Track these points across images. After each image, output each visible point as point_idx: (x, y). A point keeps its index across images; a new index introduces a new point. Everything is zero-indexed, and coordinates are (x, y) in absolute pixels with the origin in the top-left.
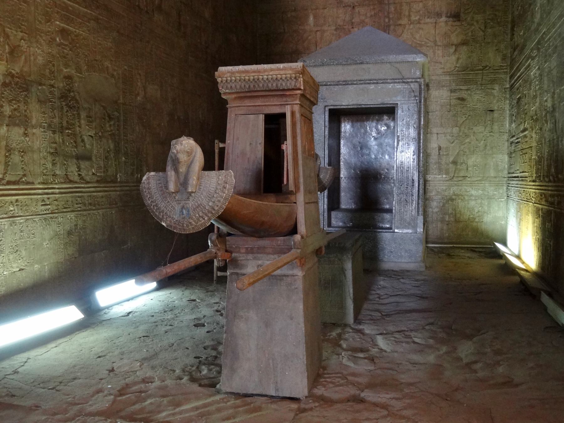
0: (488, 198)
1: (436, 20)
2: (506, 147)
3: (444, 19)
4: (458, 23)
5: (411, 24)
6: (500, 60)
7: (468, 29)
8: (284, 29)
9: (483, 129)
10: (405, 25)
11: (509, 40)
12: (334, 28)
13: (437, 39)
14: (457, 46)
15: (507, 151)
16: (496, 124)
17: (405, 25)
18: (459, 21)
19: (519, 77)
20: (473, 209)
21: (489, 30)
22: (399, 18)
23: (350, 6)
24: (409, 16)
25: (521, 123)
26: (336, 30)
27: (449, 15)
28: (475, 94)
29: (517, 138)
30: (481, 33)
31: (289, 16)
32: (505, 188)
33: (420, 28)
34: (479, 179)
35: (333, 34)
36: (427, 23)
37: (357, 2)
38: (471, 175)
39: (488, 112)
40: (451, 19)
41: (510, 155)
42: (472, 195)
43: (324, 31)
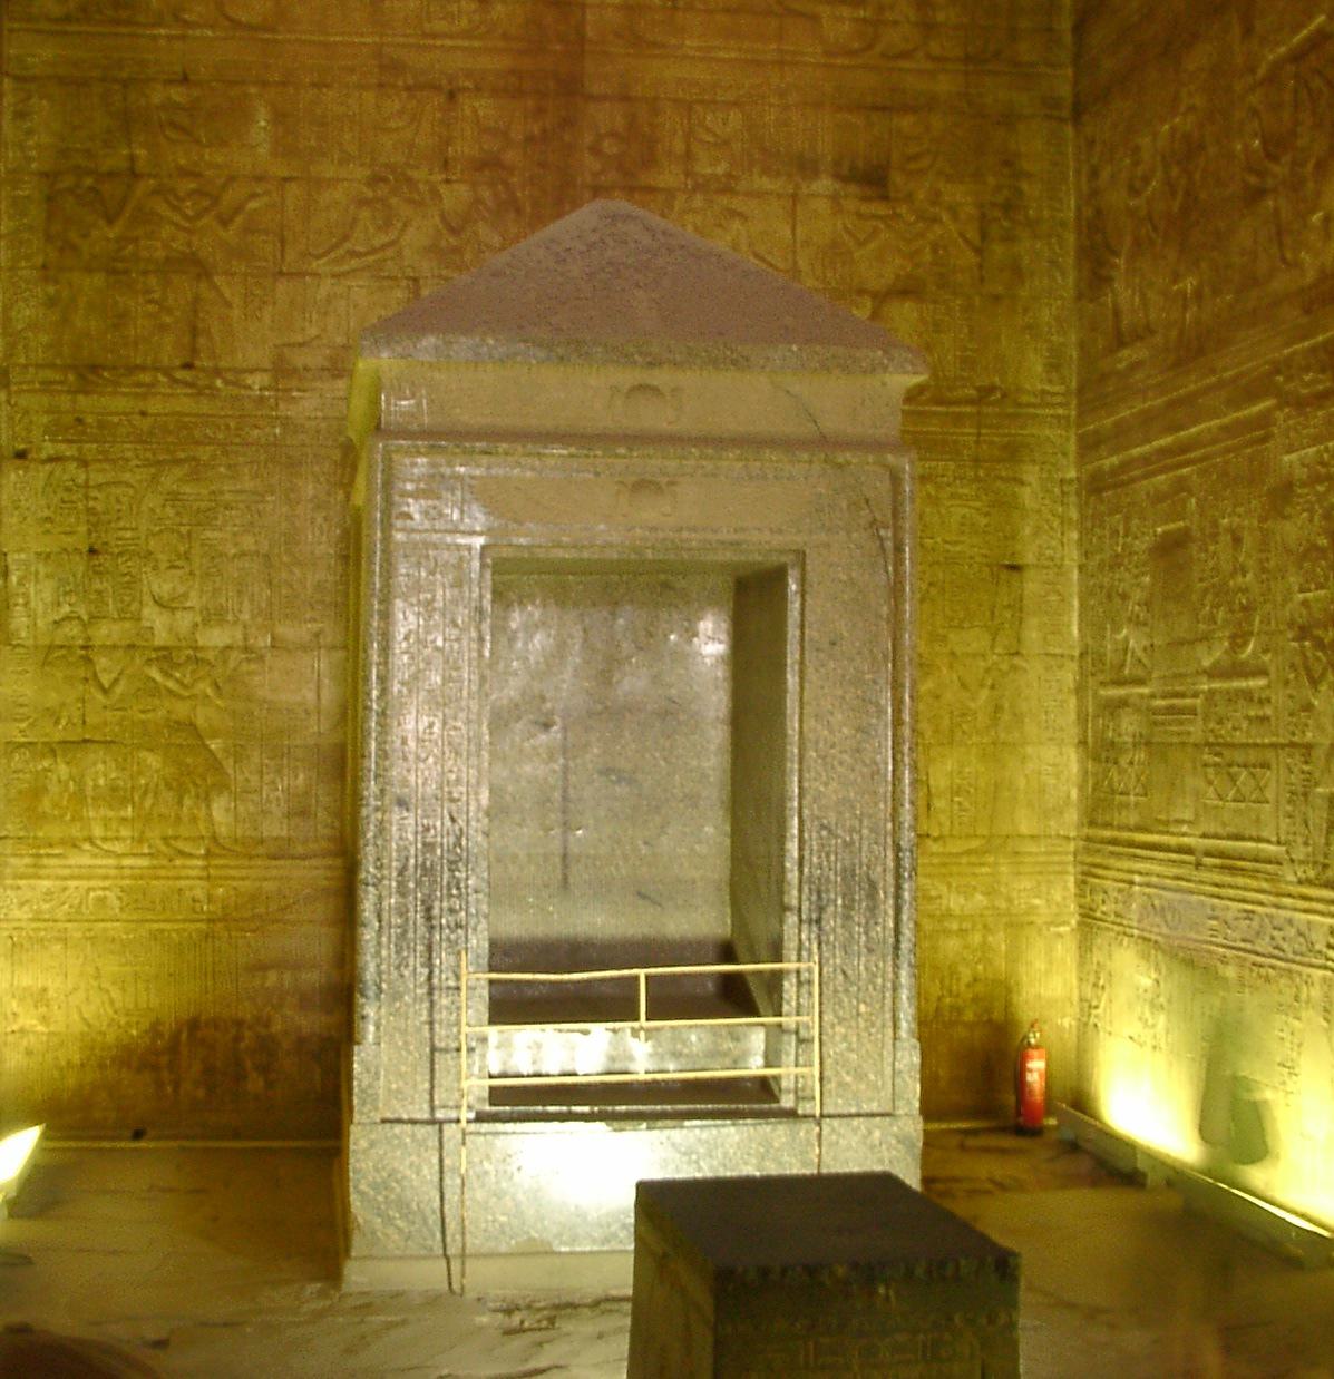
0: (1010, 925)
1: (797, 187)
2: (1073, 716)
3: (824, 184)
4: (881, 209)
5: (697, 188)
6: (1039, 368)
7: (922, 235)
8: (132, 158)
9: (985, 640)
10: (670, 194)
11: (1069, 293)
12: (362, 173)
13: (803, 263)
14: (875, 296)
15: (1073, 732)
16: (1033, 621)
17: (670, 194)
18: (885, 198)
19: (1164, 452)
20: (953, 972)
21: (998, 250)
22: (649, 161)
23: (437, 88)
24: (688, 156)
25: (1206, 638)
26: (375, 180)
27: (845, 170)
28: (953, 496)
29: (1182, 695)
30: (970, 258)
31: (157, 96)
32: (1071, 879)
33: (734, 213)
34: (975, 844)
35: (363, 202)
36: (760, 195)
37: (469, 74)
38: (946, 833)
39: (1004, 575)
40: (853, 189)
41: (1100, 752)
42: (949, 914)
43: (320, 183)
